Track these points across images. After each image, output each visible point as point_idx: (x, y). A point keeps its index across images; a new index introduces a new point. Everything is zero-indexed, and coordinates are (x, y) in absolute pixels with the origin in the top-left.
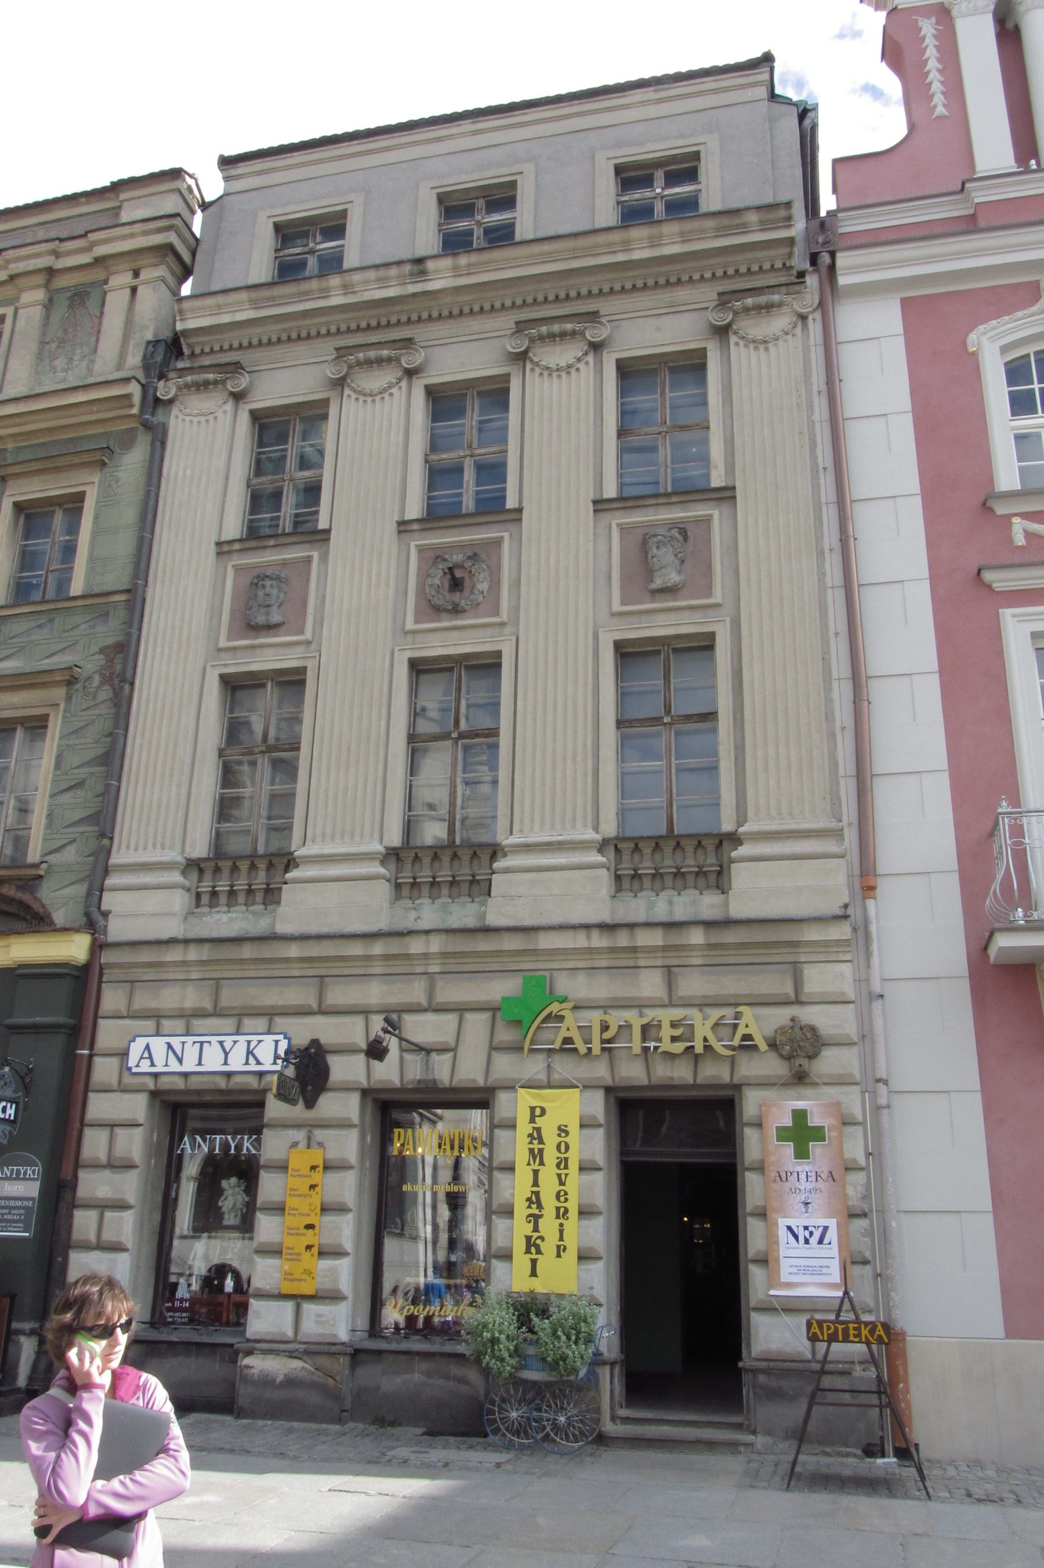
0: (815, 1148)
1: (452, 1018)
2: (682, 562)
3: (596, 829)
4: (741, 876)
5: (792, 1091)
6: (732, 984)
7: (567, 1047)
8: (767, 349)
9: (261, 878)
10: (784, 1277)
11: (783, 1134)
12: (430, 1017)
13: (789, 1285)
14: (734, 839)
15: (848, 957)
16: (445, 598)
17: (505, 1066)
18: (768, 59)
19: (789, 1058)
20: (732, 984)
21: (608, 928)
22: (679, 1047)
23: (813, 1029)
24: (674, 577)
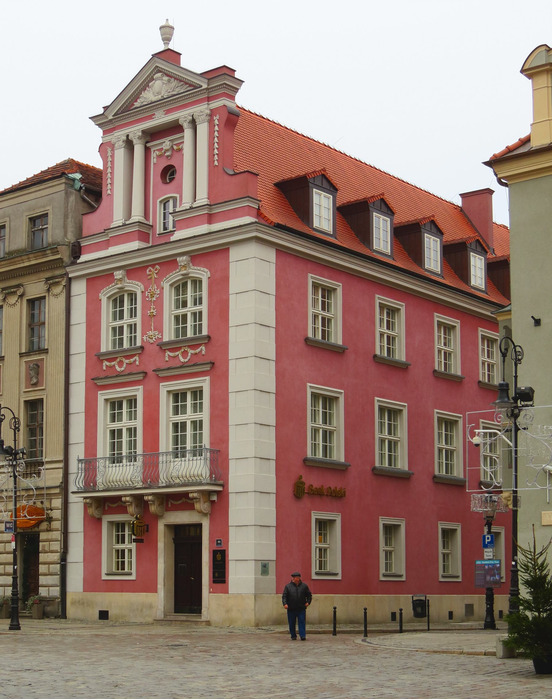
24: (34, 380)
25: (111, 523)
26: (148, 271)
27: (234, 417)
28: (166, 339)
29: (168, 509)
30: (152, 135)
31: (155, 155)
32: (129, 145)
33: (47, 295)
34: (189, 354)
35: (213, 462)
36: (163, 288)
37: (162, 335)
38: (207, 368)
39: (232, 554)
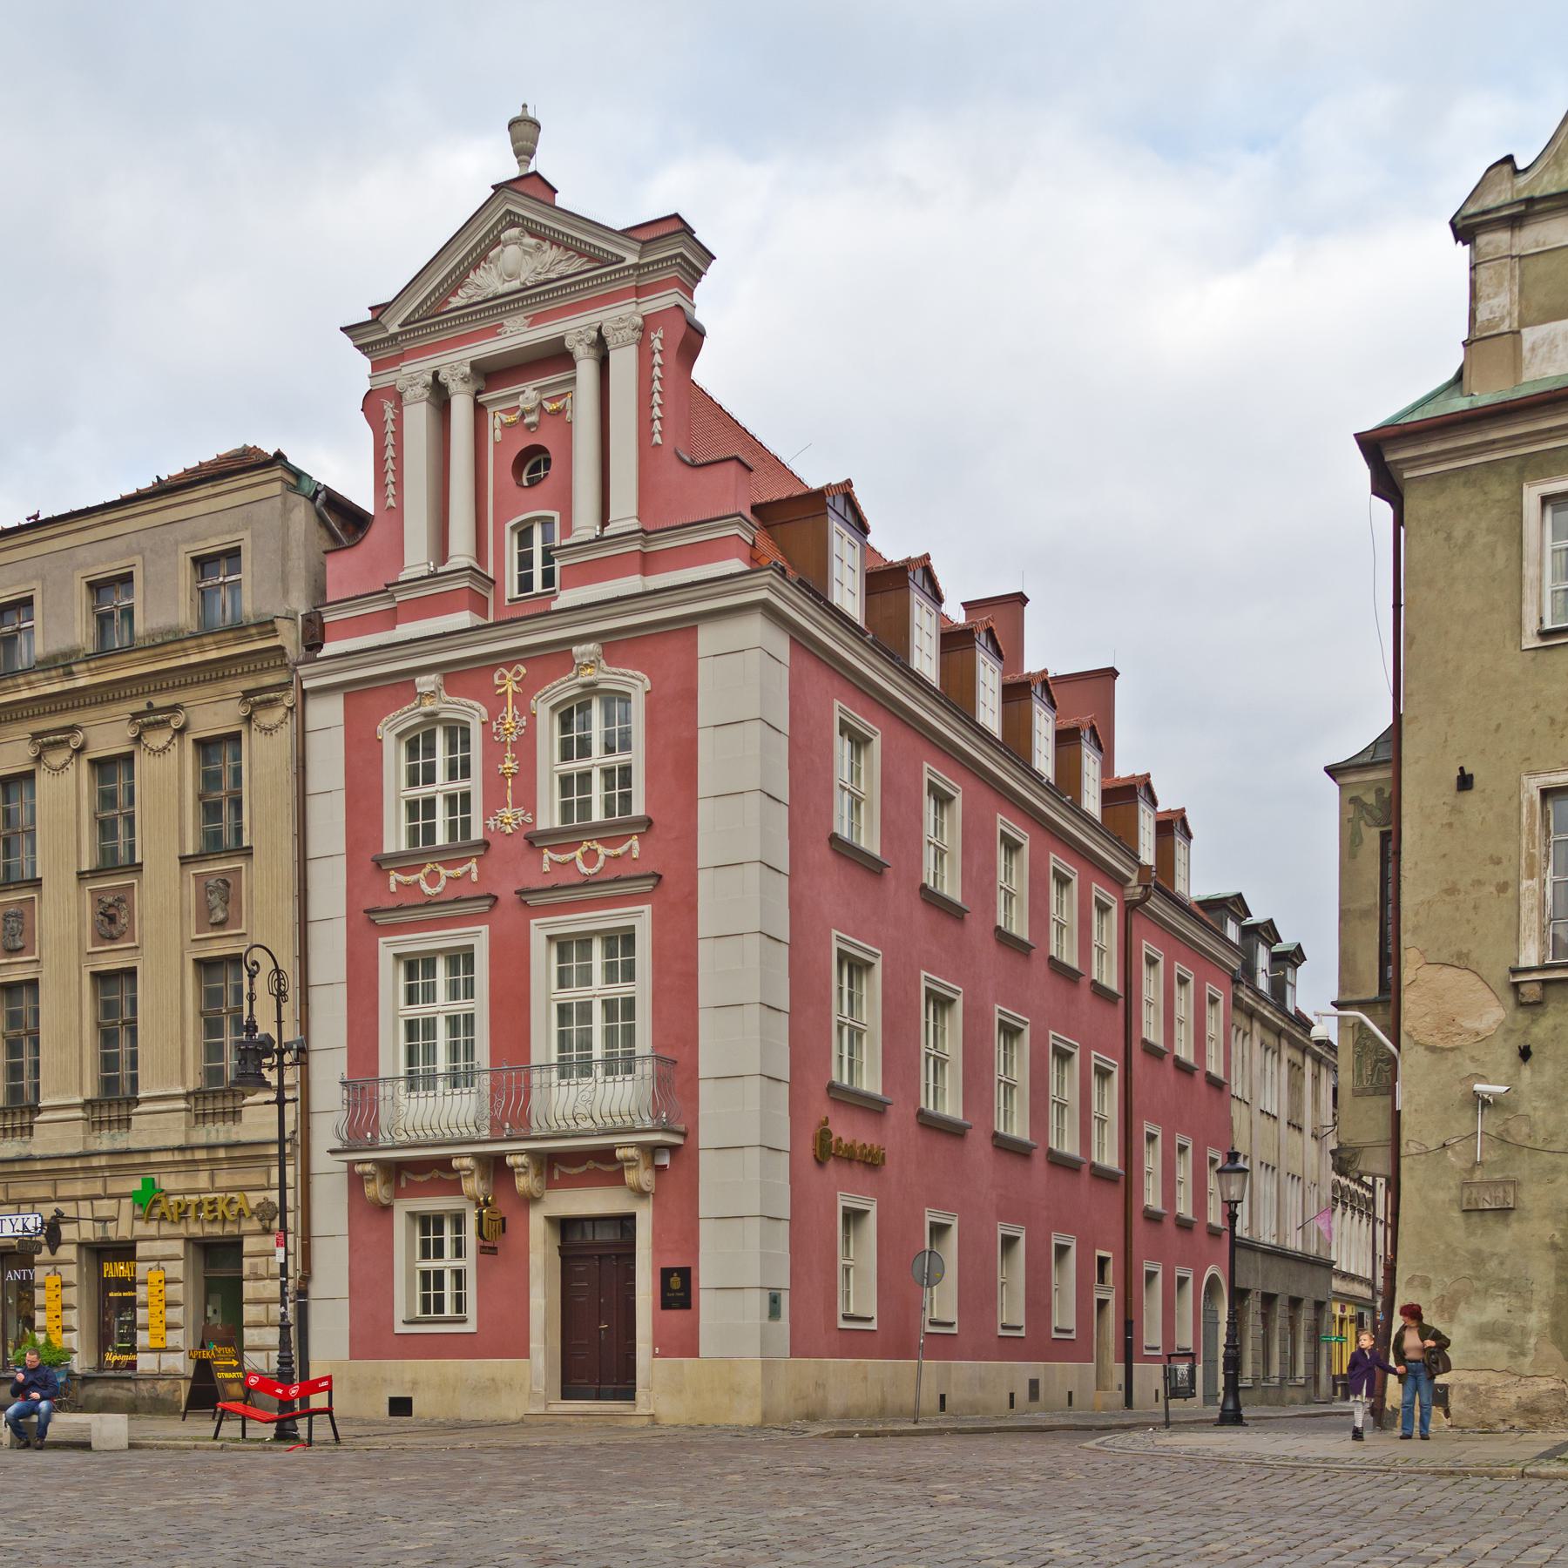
1: (114, 1201)
3: (183, 1083)
6: (240, 1179)
7: (163, 1217)
9: (27, 1118)
12: (105, 1202)
16: (107, 928)
17: (141, 1228)
20: (240, 1179)
21: (181, 1149)
22: (211, 1217)
24: (220, 915)
26: (496, 676)
27: (708, 992)
28: (543, 824)
29: (551, 1185)
33: (244, 729)
34: (602, 858)
35: (662, 1082)
37: (534, 817)
38: (646, 886)
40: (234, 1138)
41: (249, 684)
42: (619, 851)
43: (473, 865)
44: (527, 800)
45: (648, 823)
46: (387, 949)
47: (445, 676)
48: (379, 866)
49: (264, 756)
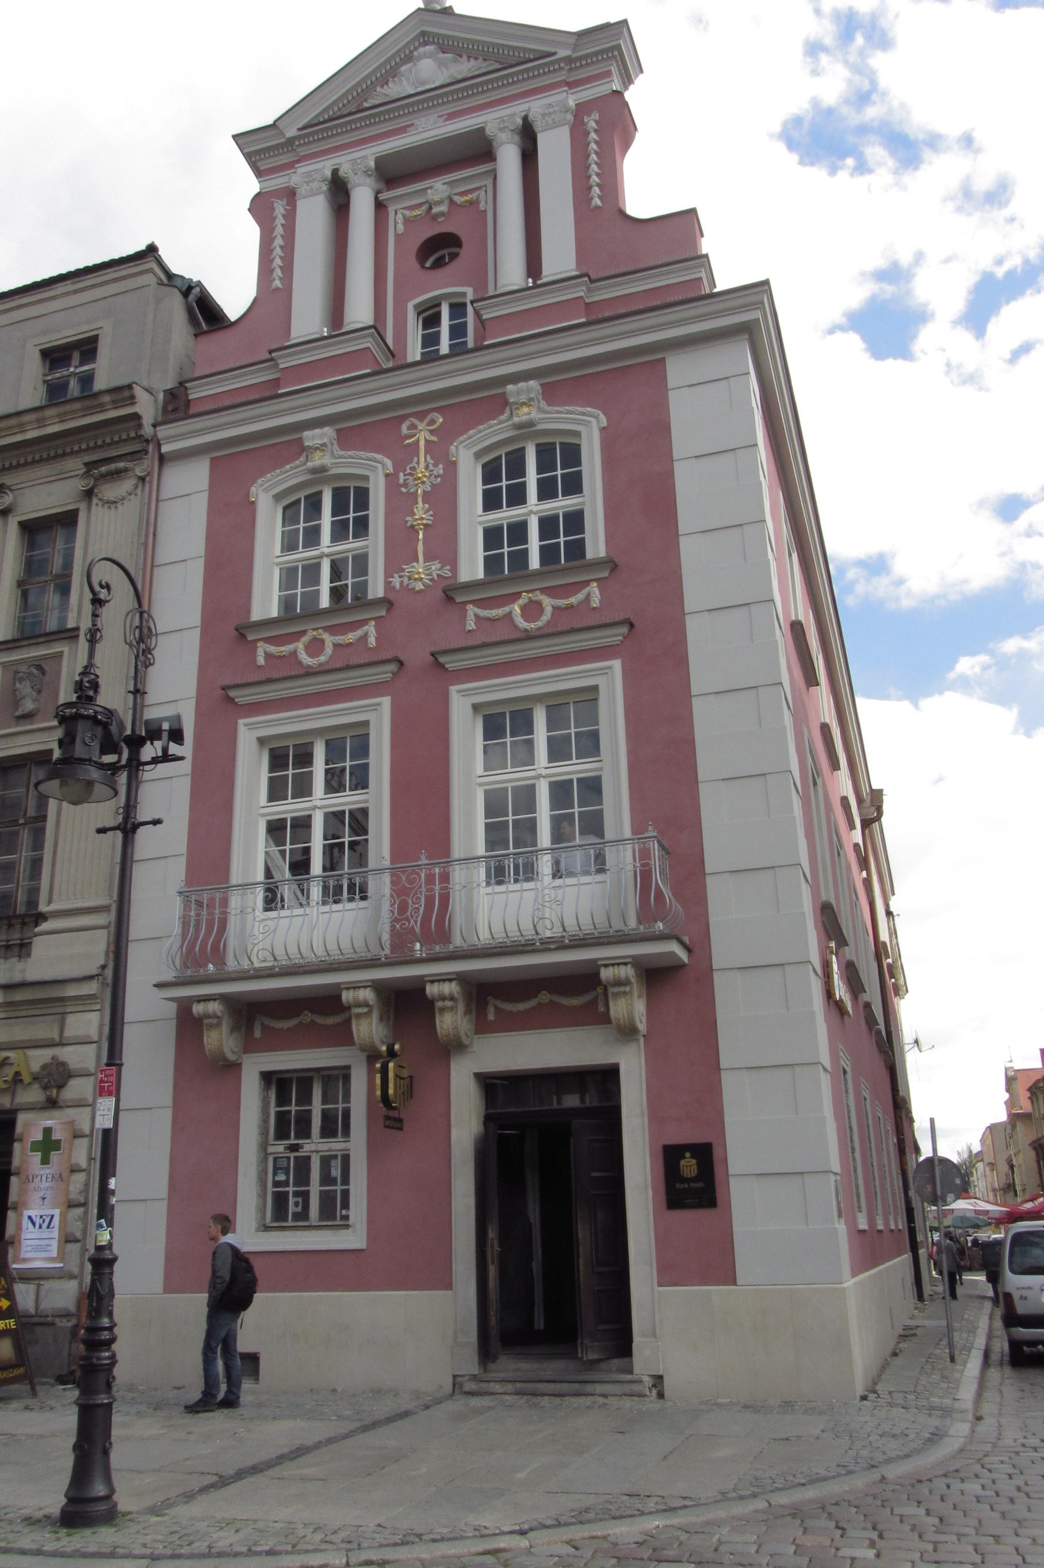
0: (54, 1156)
2: (39, 692)
4: (40, 946)
5: (47, 1114)
8: (116, 508)
10: (23, 1255)
11: (35, 1146)
13: (25, 1260)
14: (41, 917)
15: (98, 1007)
18: (152, 249)
19: (45, 1088)
23: (64, 1064)
24: (29, 706)
25: (267, 1077)
29: (482, 1027)
30: (392, 174)
31: (400, 216)
32: (339, 192)
33: (82, 507)
36: (455, 463)
37: (454, 570)
38: (615, 636)
39: (740, 1157)
40: (17, 978)
41: (88, 458)
42: (573, 600)
43: (371, 628)
44: (445, 549)
45: (610, 564)
46: (248, 735)
47: (339, 432)
48: (243, 636)
49: (104, 532)
